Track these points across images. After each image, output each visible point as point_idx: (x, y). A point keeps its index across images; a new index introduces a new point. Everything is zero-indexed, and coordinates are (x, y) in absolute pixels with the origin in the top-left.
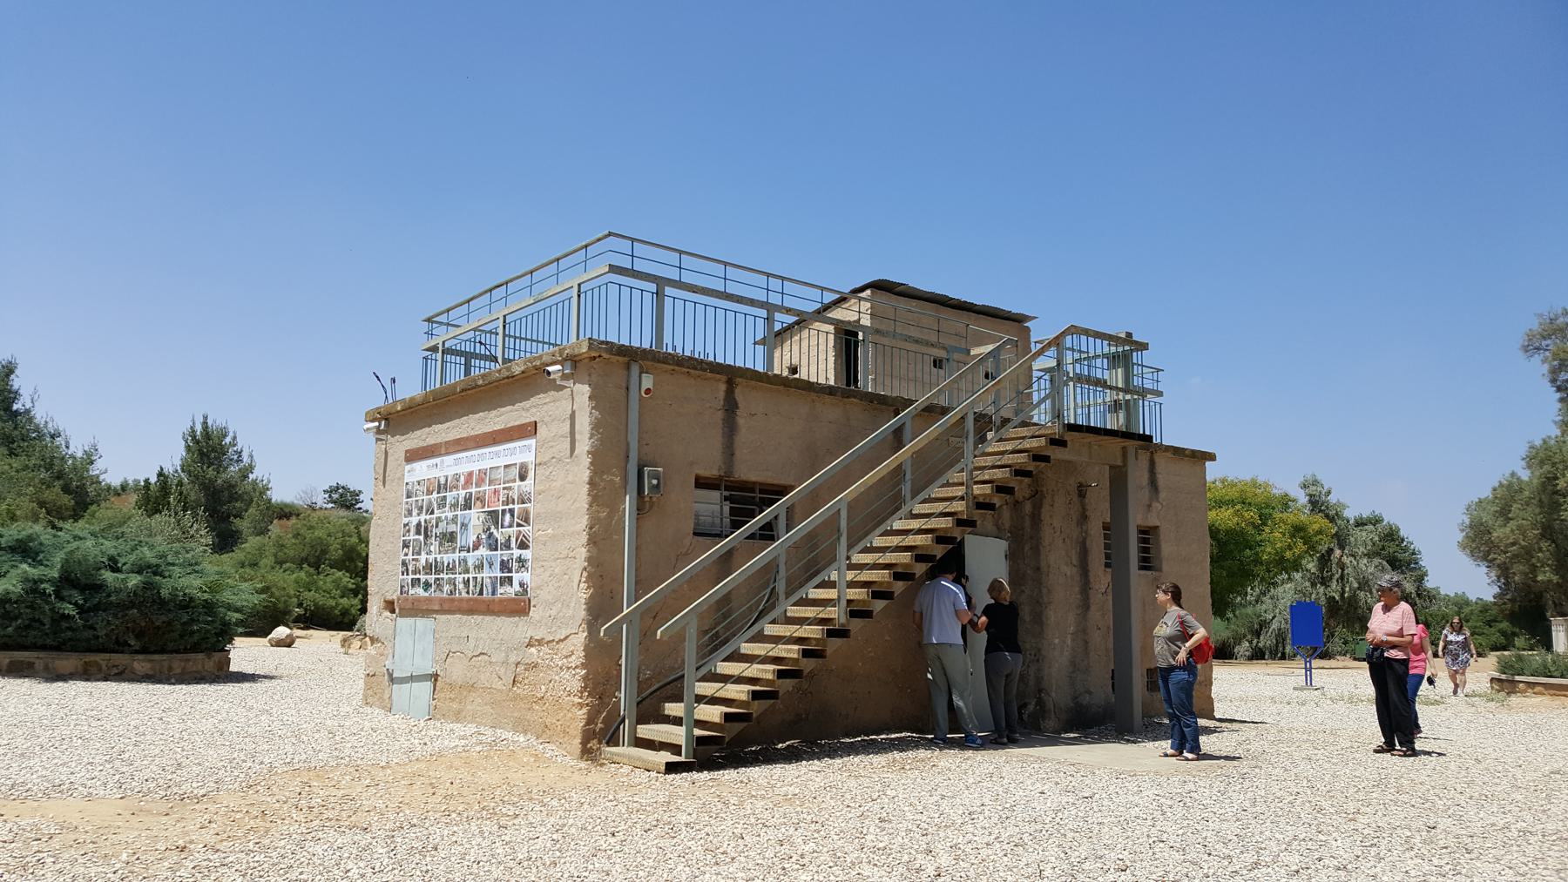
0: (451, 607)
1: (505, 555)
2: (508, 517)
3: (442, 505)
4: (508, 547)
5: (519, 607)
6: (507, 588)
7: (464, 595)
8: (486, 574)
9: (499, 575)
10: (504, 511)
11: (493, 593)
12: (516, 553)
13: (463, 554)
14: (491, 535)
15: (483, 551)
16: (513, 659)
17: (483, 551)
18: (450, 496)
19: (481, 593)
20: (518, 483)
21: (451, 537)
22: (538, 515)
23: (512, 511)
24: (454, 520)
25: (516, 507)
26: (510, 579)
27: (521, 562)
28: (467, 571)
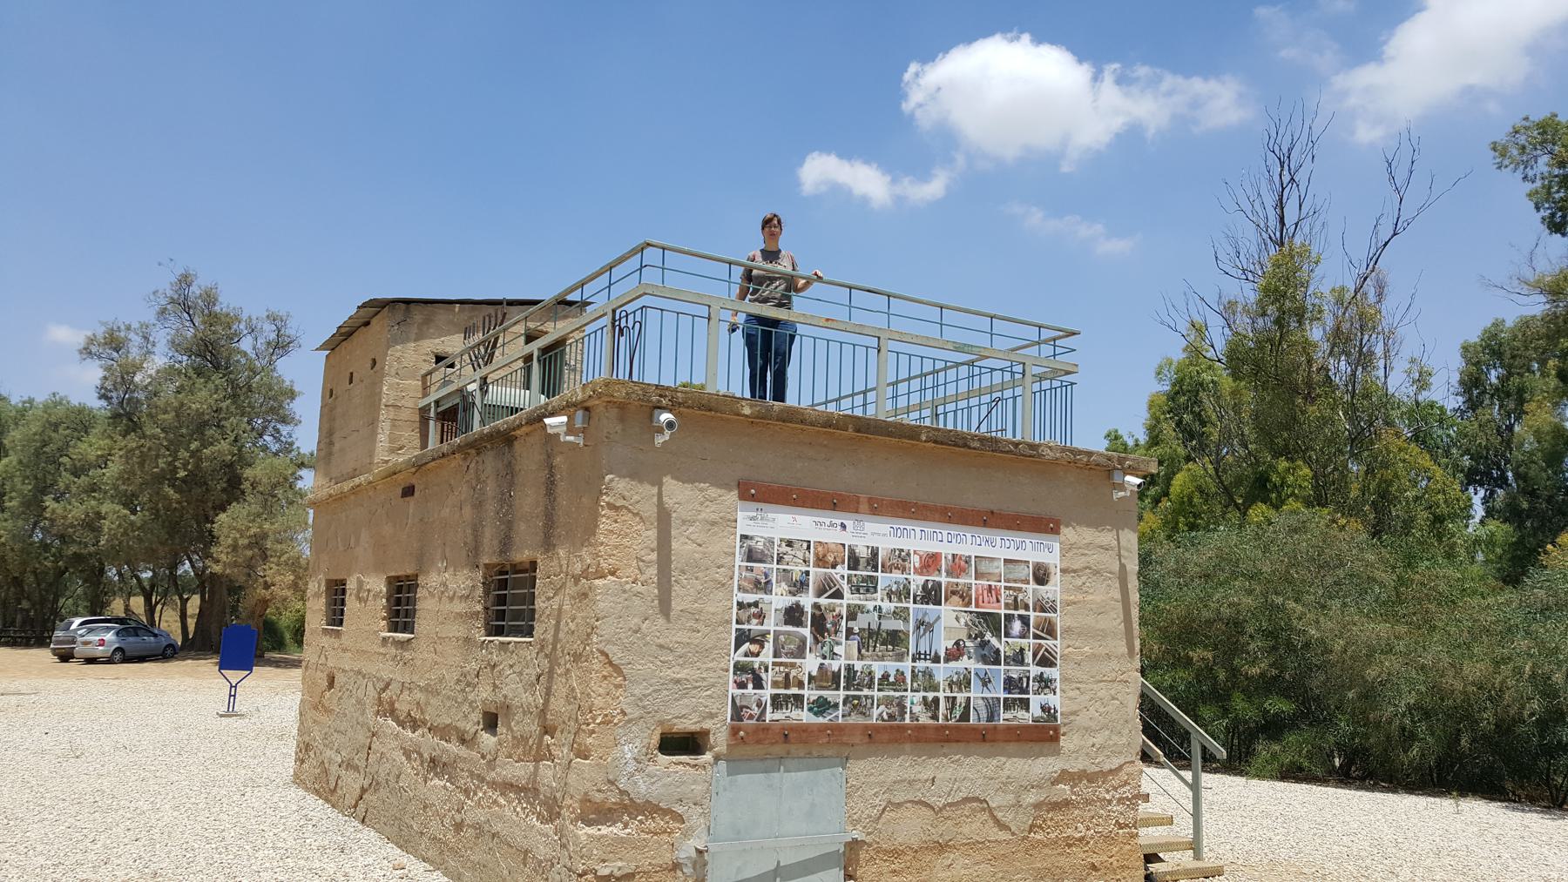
0: (895, 736)
1: (1015, 671)
2: (1017, 626)
3: (870, 586)
4: (1021, 662)
5: (1044, 734)
6: (1021, 714)
7: (925, 719)
8: (976, 693)
9: (1002, 695)
10: (1009, 618)
11: (991, 718)
12: (1035, 670)
13: (921, 665)
14: (984, 644)
15: (968, 663)
16: (1031, 798)
17: (968, 663)
18: (884, 579)
19: (965, 716)
20: (1032, 586)
21: (895, 639)
22: (1067, 631)
23: (1025, 620)
24: (900, 614)
25: (1032, 615)
26: (1025, 704)
27: (1045, 684)
28: (936, 688)
